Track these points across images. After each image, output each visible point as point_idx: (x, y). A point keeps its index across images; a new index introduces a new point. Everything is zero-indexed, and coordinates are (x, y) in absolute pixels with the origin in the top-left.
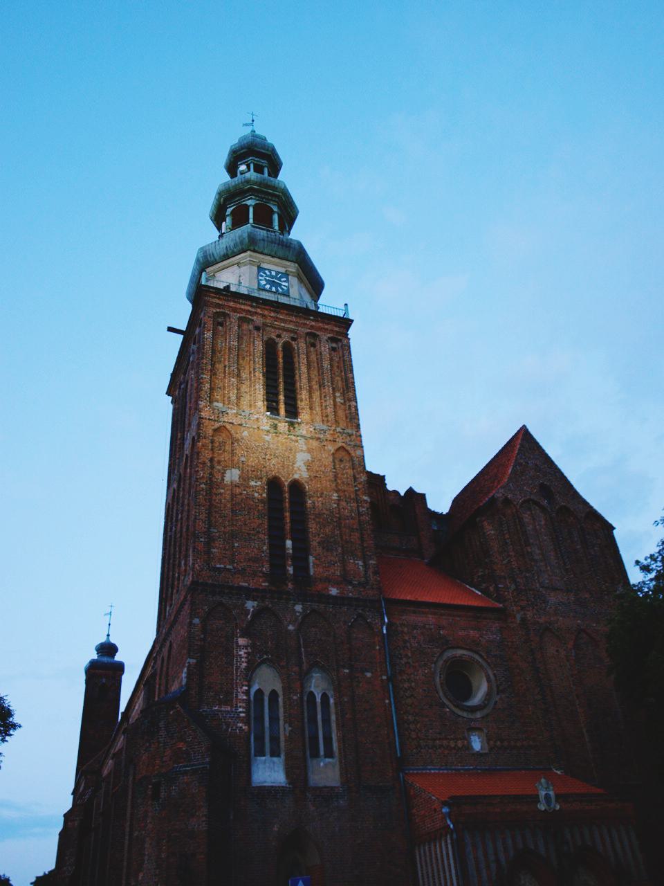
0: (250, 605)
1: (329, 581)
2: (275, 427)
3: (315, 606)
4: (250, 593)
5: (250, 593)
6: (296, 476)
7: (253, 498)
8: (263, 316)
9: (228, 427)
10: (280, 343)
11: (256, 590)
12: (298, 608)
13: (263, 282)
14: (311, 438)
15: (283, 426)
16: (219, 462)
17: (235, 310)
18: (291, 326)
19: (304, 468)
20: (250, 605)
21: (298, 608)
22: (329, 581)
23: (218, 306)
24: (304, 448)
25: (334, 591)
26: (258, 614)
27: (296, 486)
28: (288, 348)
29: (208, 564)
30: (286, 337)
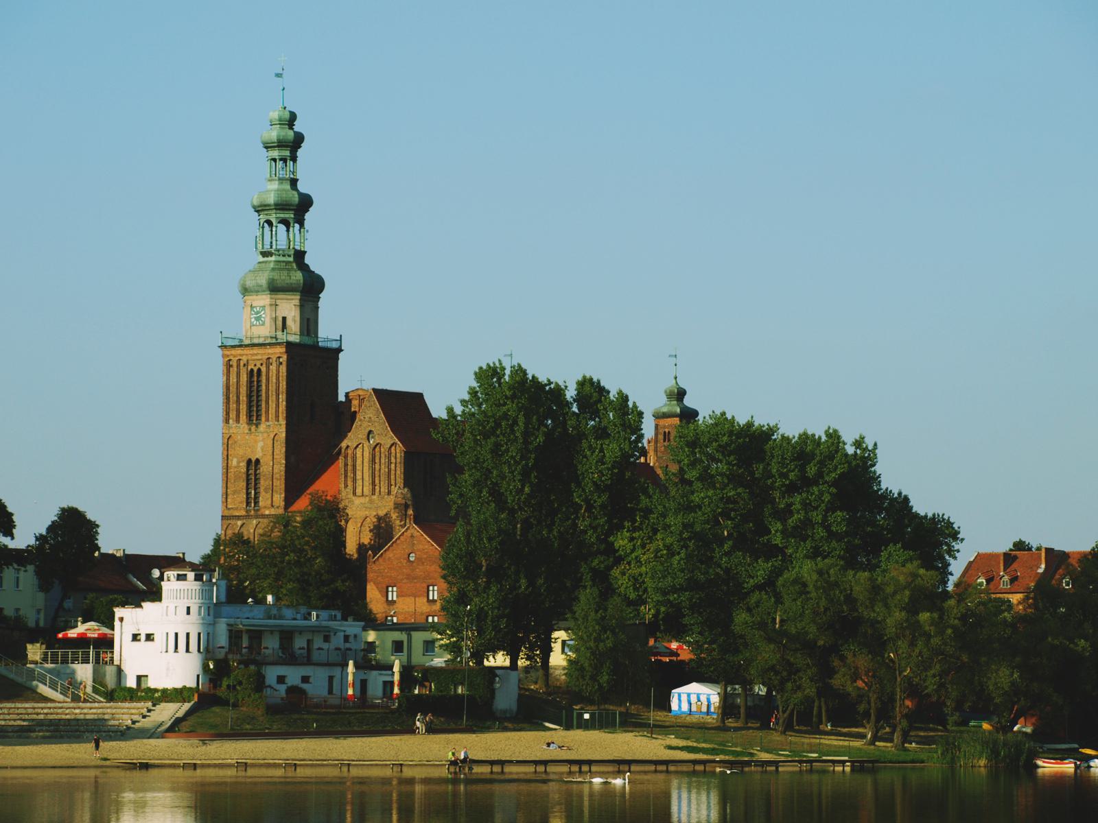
0: (239, 523)
1: (265, 507)
2: (250, 430)
3: (260, 520)
4: (238, 518)
5: (238, 518)
6: (257, 457)
7: (240, 472)
8: (247, 355)
9: (233, 435)
10: (255, 370)
11: (241, 516)
12: (255, 522)
13: (253, 320)
14: (264, 432)
15: (253, 428)
16: (231, 455)
17: (235, 357)
18: (259, 357)
19: (260, 451)
20: (239, 523)
21: (255, 522)
22: (265, 507)
23: (228, 356)
24: (261, 439)
25: (267, 512)
26: (242, 526)
27: (258, 461)
28: (259, 370)
29: (227, 507)
30: (258, 366)
